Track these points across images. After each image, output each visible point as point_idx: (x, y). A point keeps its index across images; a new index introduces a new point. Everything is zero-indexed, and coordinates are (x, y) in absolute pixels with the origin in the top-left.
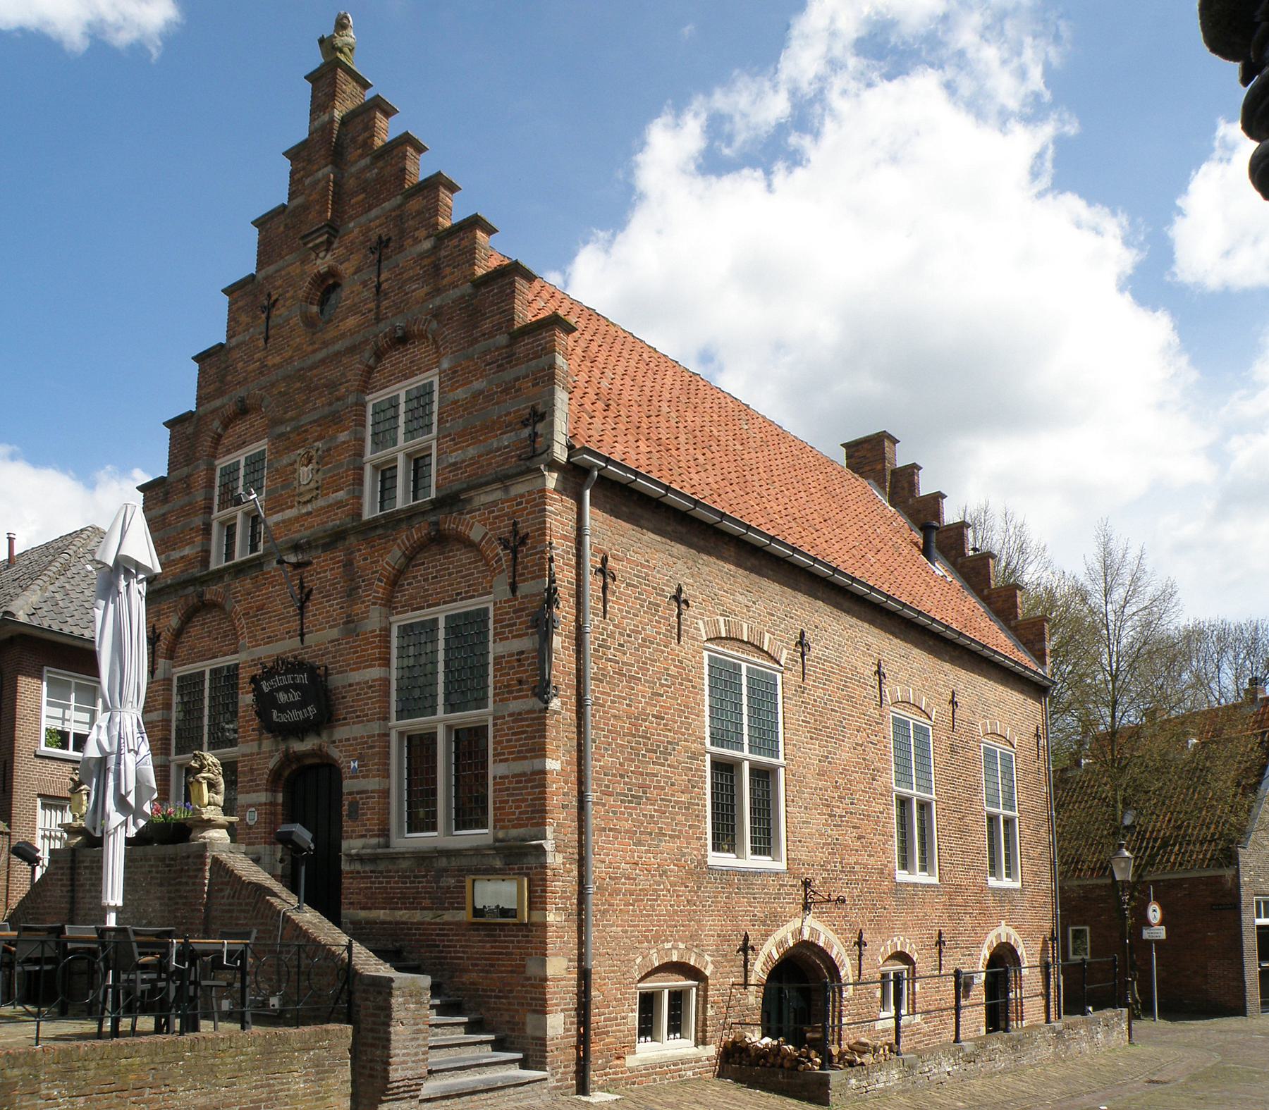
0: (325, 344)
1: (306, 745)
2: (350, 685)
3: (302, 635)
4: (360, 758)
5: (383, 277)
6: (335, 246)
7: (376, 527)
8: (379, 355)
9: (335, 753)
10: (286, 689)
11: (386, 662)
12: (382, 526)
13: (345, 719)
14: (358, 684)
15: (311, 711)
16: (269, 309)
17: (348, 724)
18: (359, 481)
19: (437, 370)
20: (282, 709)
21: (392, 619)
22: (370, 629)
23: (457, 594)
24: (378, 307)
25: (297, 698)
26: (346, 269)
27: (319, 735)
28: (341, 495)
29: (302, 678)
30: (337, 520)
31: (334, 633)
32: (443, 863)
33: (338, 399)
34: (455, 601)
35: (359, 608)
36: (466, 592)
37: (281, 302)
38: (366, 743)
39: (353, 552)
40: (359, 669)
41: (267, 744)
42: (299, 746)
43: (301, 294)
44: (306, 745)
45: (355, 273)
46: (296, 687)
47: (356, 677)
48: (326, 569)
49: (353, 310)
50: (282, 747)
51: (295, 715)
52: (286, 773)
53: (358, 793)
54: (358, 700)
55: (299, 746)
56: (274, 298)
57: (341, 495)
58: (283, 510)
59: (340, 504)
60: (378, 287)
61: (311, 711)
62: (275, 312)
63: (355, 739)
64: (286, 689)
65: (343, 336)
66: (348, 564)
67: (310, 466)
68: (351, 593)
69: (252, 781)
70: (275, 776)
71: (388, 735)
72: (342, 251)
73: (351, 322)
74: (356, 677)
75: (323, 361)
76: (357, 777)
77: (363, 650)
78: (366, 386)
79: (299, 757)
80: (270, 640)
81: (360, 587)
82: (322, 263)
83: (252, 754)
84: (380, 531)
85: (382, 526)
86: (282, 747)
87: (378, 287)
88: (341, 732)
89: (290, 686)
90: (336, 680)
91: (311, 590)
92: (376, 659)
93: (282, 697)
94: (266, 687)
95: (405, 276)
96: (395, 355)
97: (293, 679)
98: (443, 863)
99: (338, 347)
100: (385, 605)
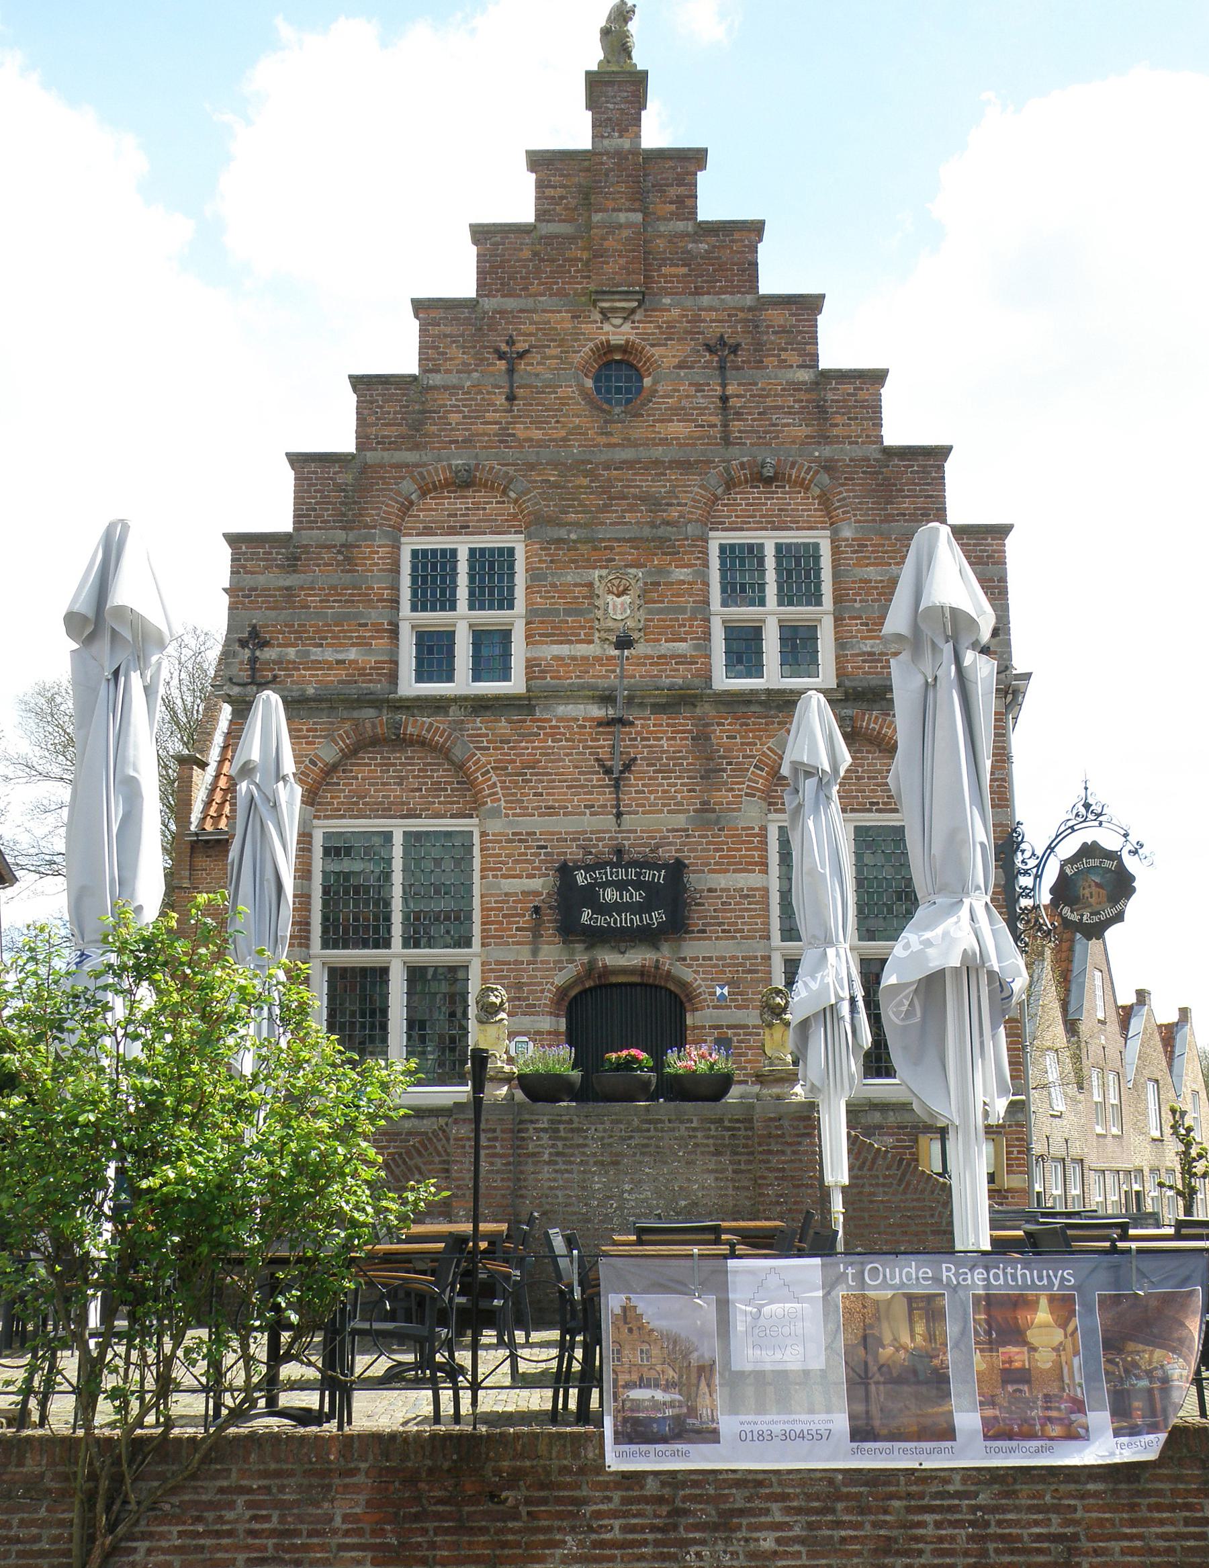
0: (629, 443)
1: (636, 958)
2: (710, 890)
3: (619, 815)
4: (731, 983)
5: (730, 390)
6: (637, 317)
7: (750, 702)
8: (730, 484)
9: (687, 975)
10: (621, 886)
11: (764, 865)
12: (761, 703)
13: (704, 931)
14: (722, 890)
15: (657, 917)
16: (513, 359)
17: (710, 938)
18: (707, 636)
19: (828, 533)
20: (603, 909)
21: (770, 816)
22: (742, 824)
23: (872, 804)
24: (725, 426)
25: (637, 898)
26: (666, 356)
27: (656, 947)
28: (682, 647)
29: (660, 877)
30: (678, 677)
31: (680, 820)
32: (877, 1118)
33: (668, 523)
34: (870, 811)
35: (723, 797)
36: (884, 804)
37: (535, 357)
38: (741, 965)
39: (707, 725)
40: (727, 871)
41: (551, 951)
42: (610, 959)
43: (577, 359)
44: (636, 958)
45: (680, 366)
46: (639, 885)
47: (722, 881)
48: (659, 737)
49: (679, 413)
50: (586, 959)
51: (625, 920)
52: (573, 993)
53: (729, 1027)
54: (725, 911)
55: (610, 959)
56: (521, 346)
57: (682, 647)
58: (570, 642)
59: (681, 659)
60: (724, 399)
61: (657, 917)
62: (522, 366)
63: (723, 958)
64: (621, 886)
65: (664, 442)
66: (701, 738)
67: (626, 599)
68: (709, 774)
69: (519, 999)
70: (562, 992)
71: (769, 958)
72: (651, 328)
73: (677, 429)
74: (722, 881)
75: (629, 464)
76: (729, 1007)
77: (729, 849)
78: (711, 522)
79: (607, 971)
80: (551, 811)
81: (724, 770)
82: (619, 332)
83: (516, 962)
84: (754, 708)
85: (761, 703)
86: (582, 958)
87: (724, 399)
88: (693, 948)
89: (631, 883)
90: (694, 880)
91: (635, 759)
92: (756, 864)
93: (610, 895)
94: (581, 878)
95: (769, 402)
96: (755, 493)
97: (638, 874)
98: (877, 1118)
99: (658, 452)
100: (765, 799)
